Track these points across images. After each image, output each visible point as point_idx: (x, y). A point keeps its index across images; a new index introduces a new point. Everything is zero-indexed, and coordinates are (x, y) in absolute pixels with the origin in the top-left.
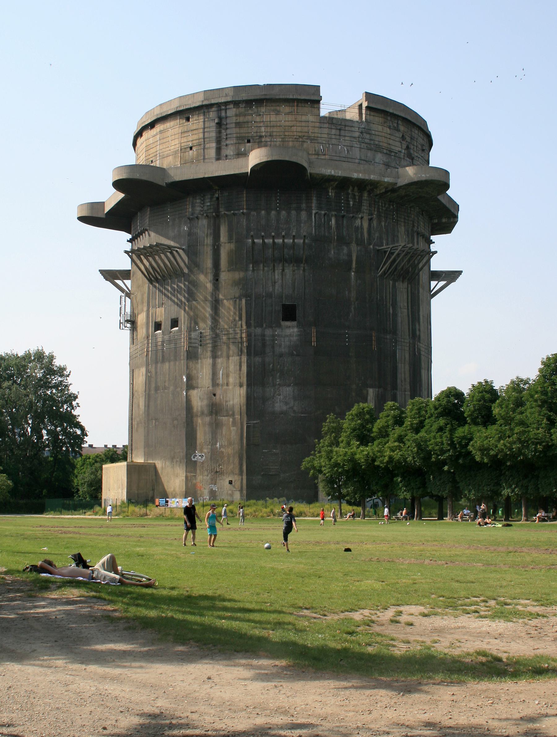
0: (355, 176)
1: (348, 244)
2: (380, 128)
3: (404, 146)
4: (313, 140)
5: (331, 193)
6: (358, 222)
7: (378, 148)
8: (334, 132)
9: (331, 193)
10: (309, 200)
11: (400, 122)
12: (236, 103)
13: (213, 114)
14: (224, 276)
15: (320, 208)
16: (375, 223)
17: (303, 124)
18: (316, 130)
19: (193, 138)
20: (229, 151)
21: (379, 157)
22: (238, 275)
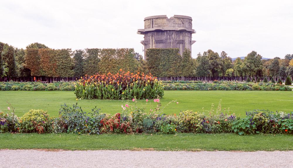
0: (171, 29)
1: (171, 39)
2: (177, 20)
4: (165, 24)
5: (168, 32)
6: (173, 36)
7: (176, 24)
9: (168, 32)
10: (165, 33)
12: (155, 18)
13: (151, 20)
14: (153, 45)
15: (166, 34)
16: (175, 36)
19: (147, 24)
20: (154, 26)
21: (177, 25)
22: (155, 45)
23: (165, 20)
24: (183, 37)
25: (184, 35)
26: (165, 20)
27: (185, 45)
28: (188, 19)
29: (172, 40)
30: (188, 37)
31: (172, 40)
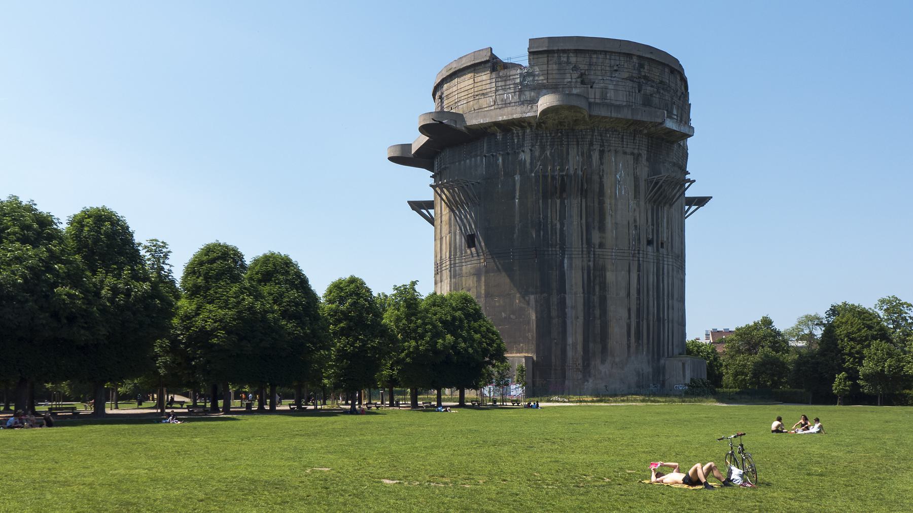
0: (500, 119)
3: (575, 75)
5: (499, 137)
6: (522, 156)
8: (500, 84)
9: (499, 137)
11: (571, 55)
17: (479, 84)
18: (488, 86)
23: (484, 77)
24: (590, 157)
25: (597, 147)
26: (484, 77)
27: (601, 203)
28: (629, 56)
29: (517, 177)
30: (630, 159)
31: (517, 177)
